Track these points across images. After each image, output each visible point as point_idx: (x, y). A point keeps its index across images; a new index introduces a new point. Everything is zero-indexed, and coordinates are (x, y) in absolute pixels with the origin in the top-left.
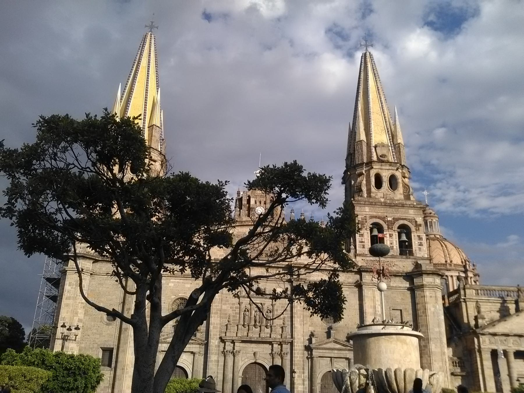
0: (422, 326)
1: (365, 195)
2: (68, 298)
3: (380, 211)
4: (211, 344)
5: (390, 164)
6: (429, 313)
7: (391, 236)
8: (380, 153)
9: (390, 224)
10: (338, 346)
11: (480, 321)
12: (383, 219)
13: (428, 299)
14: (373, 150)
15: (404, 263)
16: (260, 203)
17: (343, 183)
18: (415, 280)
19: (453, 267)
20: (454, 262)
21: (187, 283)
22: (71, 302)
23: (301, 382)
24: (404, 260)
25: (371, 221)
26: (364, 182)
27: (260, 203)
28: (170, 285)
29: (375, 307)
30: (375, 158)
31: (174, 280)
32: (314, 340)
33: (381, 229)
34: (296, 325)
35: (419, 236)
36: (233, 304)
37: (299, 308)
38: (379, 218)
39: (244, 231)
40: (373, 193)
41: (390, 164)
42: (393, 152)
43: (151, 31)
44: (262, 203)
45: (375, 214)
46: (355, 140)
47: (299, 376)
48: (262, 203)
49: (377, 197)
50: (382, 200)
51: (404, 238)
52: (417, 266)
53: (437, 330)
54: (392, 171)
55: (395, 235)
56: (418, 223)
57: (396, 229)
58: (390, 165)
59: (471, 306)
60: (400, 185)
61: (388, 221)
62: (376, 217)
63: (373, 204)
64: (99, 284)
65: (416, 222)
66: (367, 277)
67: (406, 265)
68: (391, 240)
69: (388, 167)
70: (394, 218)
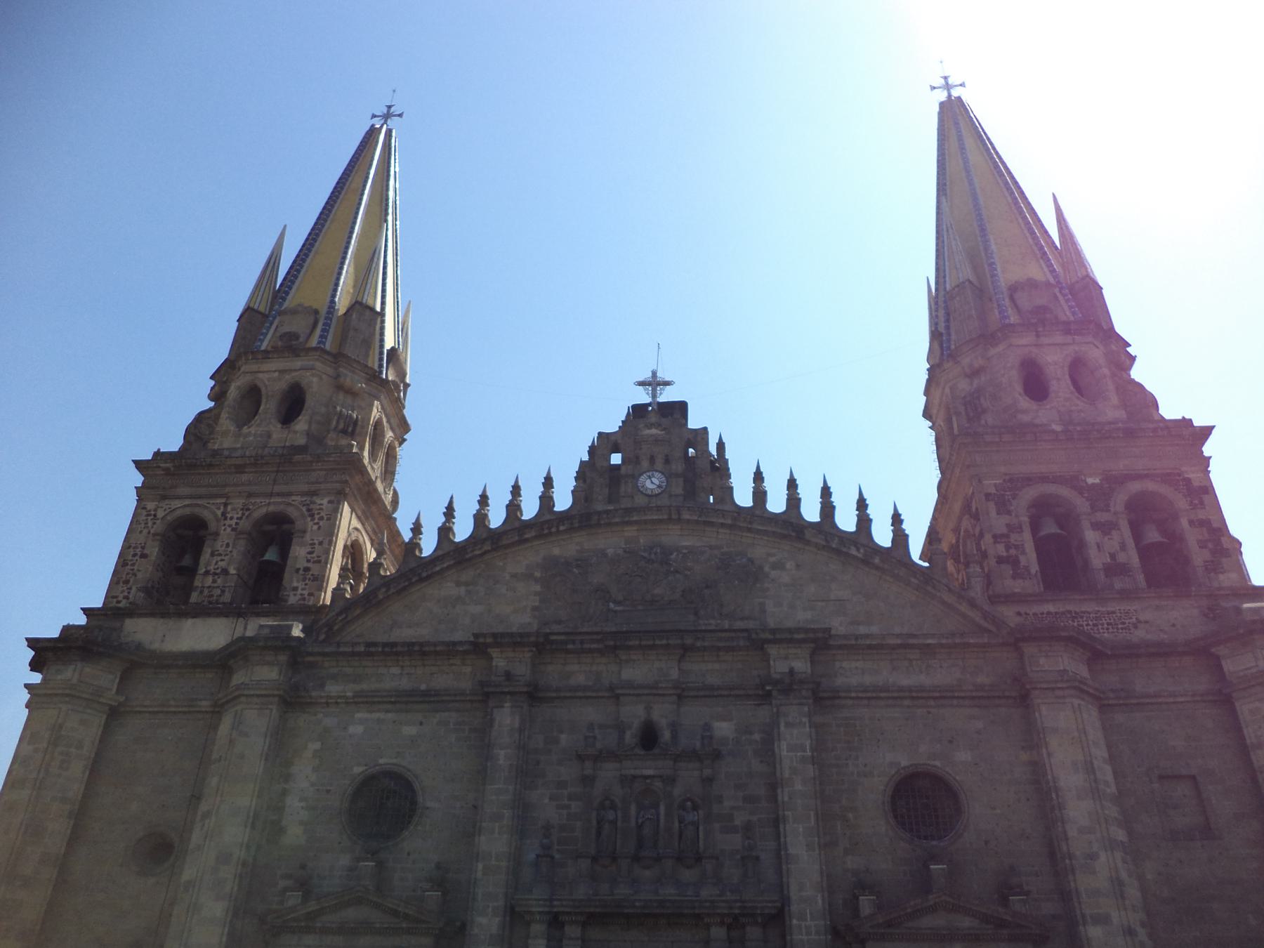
4: (476, 931)
5: (1067, 329)
10: (966, 922)
12: (1073, 482)
16: (652, 460)
18: (1228, 666)
27: (652, 460)
28: (352, 729)
29: (1089, 768)
31: (366, 715)
32: (866, 904)
33: (1067, 519)
34: (791, 851)
37: (799, 787)
42: (1067, 301)
48: (659, 464)
49: (1037, 421)
50: (1058, 428)
56: (1196, 484)
58: (1067, 332)
65: (1188, 481)
66: (1042, 661)
69: (1059, 338)
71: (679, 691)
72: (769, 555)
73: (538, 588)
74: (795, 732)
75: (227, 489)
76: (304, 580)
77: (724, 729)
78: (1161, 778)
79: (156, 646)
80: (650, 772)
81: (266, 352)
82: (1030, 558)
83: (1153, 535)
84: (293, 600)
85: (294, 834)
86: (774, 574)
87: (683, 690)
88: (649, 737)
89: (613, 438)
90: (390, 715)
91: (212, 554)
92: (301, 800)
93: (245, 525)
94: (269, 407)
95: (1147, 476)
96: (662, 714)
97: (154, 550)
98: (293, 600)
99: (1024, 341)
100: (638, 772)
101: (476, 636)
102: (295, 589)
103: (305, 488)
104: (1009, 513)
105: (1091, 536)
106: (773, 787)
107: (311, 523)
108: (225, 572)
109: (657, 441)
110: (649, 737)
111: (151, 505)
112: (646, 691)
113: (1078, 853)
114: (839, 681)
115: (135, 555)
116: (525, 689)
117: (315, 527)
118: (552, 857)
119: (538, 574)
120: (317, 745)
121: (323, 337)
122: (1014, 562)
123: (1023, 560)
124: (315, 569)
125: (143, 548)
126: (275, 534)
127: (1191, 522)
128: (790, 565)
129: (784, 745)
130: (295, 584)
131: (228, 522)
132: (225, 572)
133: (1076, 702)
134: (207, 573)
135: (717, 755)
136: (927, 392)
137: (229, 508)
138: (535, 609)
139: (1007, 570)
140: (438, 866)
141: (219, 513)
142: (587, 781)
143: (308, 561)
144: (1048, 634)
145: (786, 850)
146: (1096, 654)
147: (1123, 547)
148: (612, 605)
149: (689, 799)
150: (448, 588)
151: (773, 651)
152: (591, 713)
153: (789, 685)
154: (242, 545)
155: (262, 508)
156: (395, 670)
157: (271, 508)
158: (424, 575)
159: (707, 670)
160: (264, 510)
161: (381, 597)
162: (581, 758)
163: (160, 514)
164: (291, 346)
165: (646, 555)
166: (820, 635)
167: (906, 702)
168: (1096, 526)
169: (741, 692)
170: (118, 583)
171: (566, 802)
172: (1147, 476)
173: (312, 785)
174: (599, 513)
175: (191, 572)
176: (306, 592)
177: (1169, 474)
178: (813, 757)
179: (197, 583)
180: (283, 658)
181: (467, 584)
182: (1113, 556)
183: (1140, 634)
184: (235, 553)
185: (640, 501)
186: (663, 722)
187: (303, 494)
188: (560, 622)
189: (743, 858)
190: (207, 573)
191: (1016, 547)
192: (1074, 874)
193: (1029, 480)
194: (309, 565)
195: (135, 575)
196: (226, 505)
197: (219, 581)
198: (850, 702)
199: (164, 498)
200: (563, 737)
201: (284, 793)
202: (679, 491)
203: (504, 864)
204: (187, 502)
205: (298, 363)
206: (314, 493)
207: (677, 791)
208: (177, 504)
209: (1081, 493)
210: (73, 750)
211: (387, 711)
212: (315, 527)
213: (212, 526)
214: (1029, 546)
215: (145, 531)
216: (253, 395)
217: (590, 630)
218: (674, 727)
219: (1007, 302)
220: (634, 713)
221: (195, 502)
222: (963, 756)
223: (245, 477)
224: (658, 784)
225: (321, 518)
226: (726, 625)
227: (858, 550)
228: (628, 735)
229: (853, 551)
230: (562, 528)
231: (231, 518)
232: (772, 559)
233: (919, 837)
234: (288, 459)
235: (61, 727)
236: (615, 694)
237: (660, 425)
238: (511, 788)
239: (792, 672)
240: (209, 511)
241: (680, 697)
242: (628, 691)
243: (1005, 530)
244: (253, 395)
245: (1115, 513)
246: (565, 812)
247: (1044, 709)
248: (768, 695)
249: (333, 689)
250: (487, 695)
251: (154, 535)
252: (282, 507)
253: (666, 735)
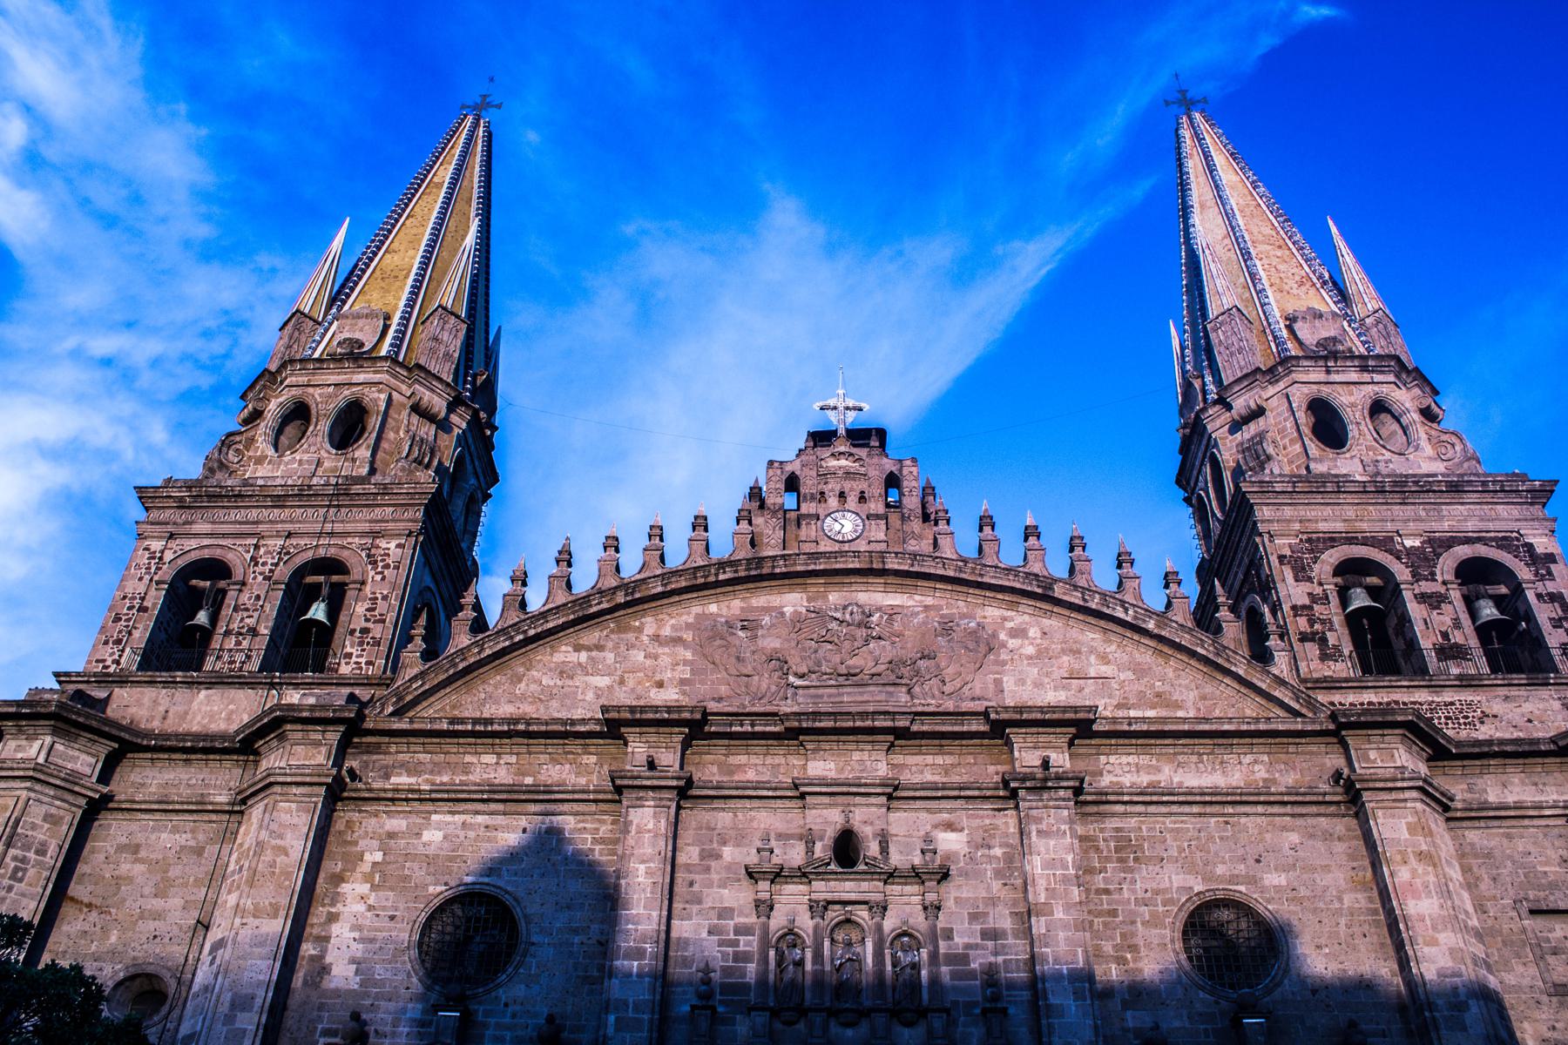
5: (1364, 364)
12: (1385, 543)
15: (1527, 707)
16: (842, 495)
21: (507, 828)
24: (1522, 692)
27: (842, 495)
28: (427, 836)
31: (448, 818)
33: (1388, 592)
36: (725, 913)
37: (1059, 914)
39: (777, 604)
40: (1320, 460)
44: (852, 501)
45: (1340, 526)
46: (1204, 316)
48: (852, 501)
51: (1489, 611)
54: (1376, 388)
56: (1540, 550)
57: (1450, 577)
58: (1364, 369)
61: (1410, 552)
62: (1351, 541)
65: (1530, 547)
70: (1430, 541)
71: (889, 790)
72: (1005, 619)
73: (689, 655)
74: (1052, 843)
75: (261, 527)
76: (361, 644)
77: (950, 842)
80: (853, 897)
81: (319, 360)
82: (1339, 636)
83: (1489, 611)
84: (345, 669)
85: (342, 974)
86: (1013, 643)
87: (896, 788)
88: (846, 849)
89: (789, 468)
90: (480, 819)
91: (236, 609)
92: (355, 928)
93: (284, 572)
95: (1479, 540)
96: (866, 818)
97: (156, 599)
98: (345, 669)
99: (1313, 377)
100: (836, 896)
101: (604, 709)
102: (349, 655)
103: (366, 527)
104: (1310, 579)
105: (1415, 610)
106: (1026, 915)
107: (372, 573)
108: (253, 632)
109: (849, 475)
110: (846, 849)
112: (845, 789)
113: (1440, 1002)
114: (1106, 781)
115: (130, 608)
116: (674, 783)
117: (378, 577)
118: (714, 1009)
119: (688, 636)
120: (378, 856)
121: (397, 345)
122: (1323, 641)
123: (1332, 639)
124: (377, 631)
125: (143, 599)
127: (1539, 596)
128: (1033, 632)
129: (1037, 860)
130: (348, 650)
131: (260, 568)
132: (253, 632)
133: (1419, 805)
134: (228, 633)
135: (945, 876)
136: (1181, 452)
137: (262, 551)
138: (683, 682)
139: (1312, 649)
140: (550, 1019)
141: (248, 556)
142: (765, 907)
143: (367, 620)
144: (1378, 722)
145: (1046, 999)
146: (1438, 751)
147: (1457, 624)
148: (791, 679)
149: (905, 934)
150: (565, 654)
151: (1018, 738)
152: (767, 819)
153: (1044, 782)
155: (308, 549)
156: (490, 759)
157: (322, 552)
158: (532, 632)
159: (922, 767)
160: (310, 555)
161: (472, 660)
162: (751, 875)
163: (168, 556)
164: (355, 355)
165: (838, 615)
166: (1081, 716)
167: (1195, 809)
168: (1422, 598)
169: (976, 793)
170: (106, 643)
171: (732, 936)
172: (1479, 540)
173: (370, 908)
174: (774, 558)
175: (207, 634)
176: (363, 660)
177: (1504, 538)
178: (1077, 877)
179: (215, 644)
180: (334, 736)
181: (589, 649)
182: (1445, 635)
183: (1485, 732)
184: (267, 607)
185: (826, 546)
186: (866, 831)
187: (363, 534)
188: (720, 700)
189: (985, 1011)
190: (228, 633)
191: (1323, 622)
192: (1437, 1029)
193: (1332, 540)
194: (370, 625)
195: (130, 633)
196: (257, 547)
197: (245, 644)
198: (1119, 808)
199: (172, 536)
200: (728, 852)
201: (333, 918)
202: (882, 536)
203: (646, 1017)
204: (206, 542)
205: (361, 378)
206: (375, 535)
207: (889, 924)
208: (194, 543)
209: (1399, 558)
210: (31, 855)
211: (477, 813)
212: (378, 577)
214: (1338, 620)
215: (147, 577)
216: (299, 413)
217: (762, 710)
218: (884, 841)
219: (1285, 333)
220: (827, 819)
221: (215, 541)
222: (1274, 879)
224: (862, 914)
225: (387, 566)
226: (950, 705)
227: (1126, 610)
228: (818, 846)
229: (1119, 613)
230: (721, 577)
231: (264, 564)
232: (1009, 625)
233: (1223, 985)
234: (342, 494)
235: (17, 821)
236: (800, 793)
237: (851, 455)
238: (655, 914)
239: (1046, 764)
241: (890, 797)
242: (817, 789)
243: (1307, 602)
244: (299, 413)
245: (1444, 583)
246: (730, 949)
247: (1380, 813)
248: (1014, 794)
249: (402, 780)
250: (619, 790)
251: (158, 583)
252: (332, 552)
253: (873, 849)
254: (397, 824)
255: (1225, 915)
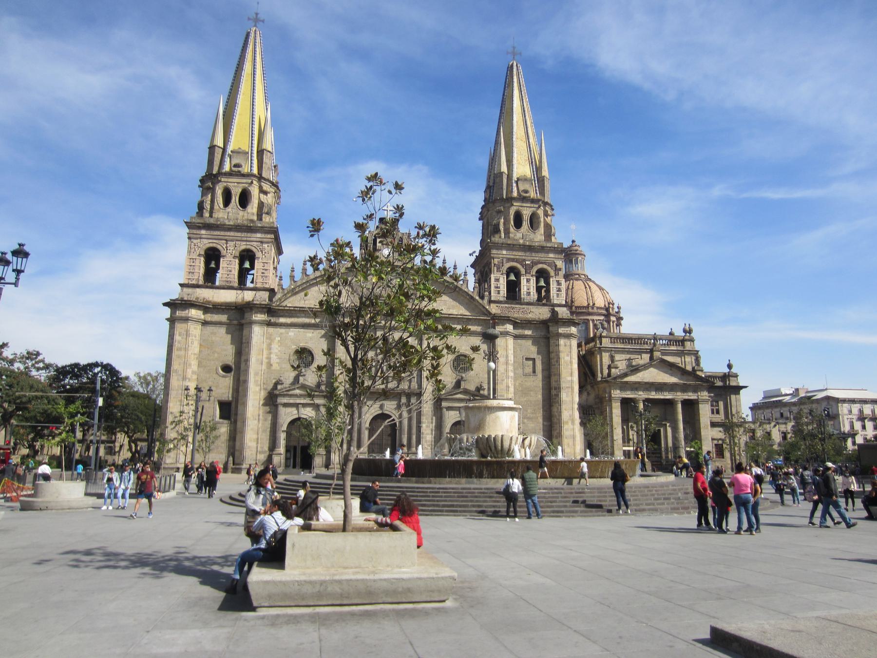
0: (555, 375)
1: (503, 235)
2: (179, 349)
3: (519, 254)
6: (562, 361)
7: (528, 281)
8: (521, 188)
9: (528, 269)
11: (613, 370)
12: (522, 262)
13: (562, 348)
14: (514, 185)
17: (480, 219)
18: (551, 329)
19: (595, 310)
20: (597, 305)
22: (182, 353)
23: (429, 432)
25: (507, 265)
26: (502, 220)
29: (507, 356)
30: (515, 194)
33: (518, 275)
35: (558, 281)
38: (517, 261)
41: (533, 201)
43: (255, 26)
47: (427, 427)
50: (521, 241)
51: (542, 283)
52: (554, 313)
53: (569, 378)
55: (533, 280)
59: (606, 357)
60: (542, 225)
62: (513, 260)
63: (511, 247)
64: (212, 333)
65: (556, 266)
67: (543, 313)
68: (528, 287)
69: (529, 205)
78: (527, 359)
79: (211, 299)
85: (275, 366)
94: (235, 199)
111: (195, 241)
126: (247, 257)
146: (516, 324)
154: (237, 261)
155: (243, 246)
183: (530, 316)
205: (244, 181)
208: (206, 241)
213: (223, 252)
223: (232, 234)
234: (248, 228)
240: (220, 245)
254: (282, 330)
255: (462, 358)
